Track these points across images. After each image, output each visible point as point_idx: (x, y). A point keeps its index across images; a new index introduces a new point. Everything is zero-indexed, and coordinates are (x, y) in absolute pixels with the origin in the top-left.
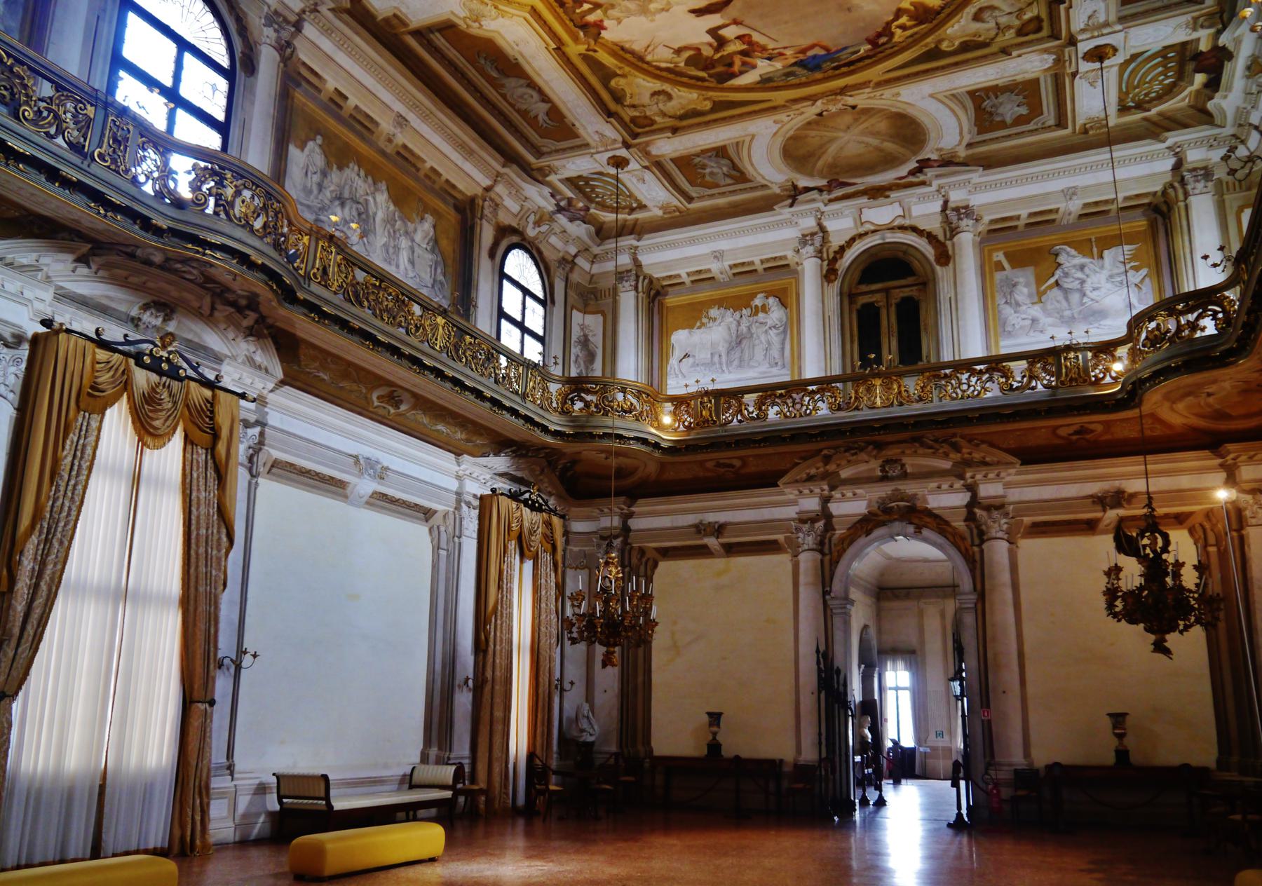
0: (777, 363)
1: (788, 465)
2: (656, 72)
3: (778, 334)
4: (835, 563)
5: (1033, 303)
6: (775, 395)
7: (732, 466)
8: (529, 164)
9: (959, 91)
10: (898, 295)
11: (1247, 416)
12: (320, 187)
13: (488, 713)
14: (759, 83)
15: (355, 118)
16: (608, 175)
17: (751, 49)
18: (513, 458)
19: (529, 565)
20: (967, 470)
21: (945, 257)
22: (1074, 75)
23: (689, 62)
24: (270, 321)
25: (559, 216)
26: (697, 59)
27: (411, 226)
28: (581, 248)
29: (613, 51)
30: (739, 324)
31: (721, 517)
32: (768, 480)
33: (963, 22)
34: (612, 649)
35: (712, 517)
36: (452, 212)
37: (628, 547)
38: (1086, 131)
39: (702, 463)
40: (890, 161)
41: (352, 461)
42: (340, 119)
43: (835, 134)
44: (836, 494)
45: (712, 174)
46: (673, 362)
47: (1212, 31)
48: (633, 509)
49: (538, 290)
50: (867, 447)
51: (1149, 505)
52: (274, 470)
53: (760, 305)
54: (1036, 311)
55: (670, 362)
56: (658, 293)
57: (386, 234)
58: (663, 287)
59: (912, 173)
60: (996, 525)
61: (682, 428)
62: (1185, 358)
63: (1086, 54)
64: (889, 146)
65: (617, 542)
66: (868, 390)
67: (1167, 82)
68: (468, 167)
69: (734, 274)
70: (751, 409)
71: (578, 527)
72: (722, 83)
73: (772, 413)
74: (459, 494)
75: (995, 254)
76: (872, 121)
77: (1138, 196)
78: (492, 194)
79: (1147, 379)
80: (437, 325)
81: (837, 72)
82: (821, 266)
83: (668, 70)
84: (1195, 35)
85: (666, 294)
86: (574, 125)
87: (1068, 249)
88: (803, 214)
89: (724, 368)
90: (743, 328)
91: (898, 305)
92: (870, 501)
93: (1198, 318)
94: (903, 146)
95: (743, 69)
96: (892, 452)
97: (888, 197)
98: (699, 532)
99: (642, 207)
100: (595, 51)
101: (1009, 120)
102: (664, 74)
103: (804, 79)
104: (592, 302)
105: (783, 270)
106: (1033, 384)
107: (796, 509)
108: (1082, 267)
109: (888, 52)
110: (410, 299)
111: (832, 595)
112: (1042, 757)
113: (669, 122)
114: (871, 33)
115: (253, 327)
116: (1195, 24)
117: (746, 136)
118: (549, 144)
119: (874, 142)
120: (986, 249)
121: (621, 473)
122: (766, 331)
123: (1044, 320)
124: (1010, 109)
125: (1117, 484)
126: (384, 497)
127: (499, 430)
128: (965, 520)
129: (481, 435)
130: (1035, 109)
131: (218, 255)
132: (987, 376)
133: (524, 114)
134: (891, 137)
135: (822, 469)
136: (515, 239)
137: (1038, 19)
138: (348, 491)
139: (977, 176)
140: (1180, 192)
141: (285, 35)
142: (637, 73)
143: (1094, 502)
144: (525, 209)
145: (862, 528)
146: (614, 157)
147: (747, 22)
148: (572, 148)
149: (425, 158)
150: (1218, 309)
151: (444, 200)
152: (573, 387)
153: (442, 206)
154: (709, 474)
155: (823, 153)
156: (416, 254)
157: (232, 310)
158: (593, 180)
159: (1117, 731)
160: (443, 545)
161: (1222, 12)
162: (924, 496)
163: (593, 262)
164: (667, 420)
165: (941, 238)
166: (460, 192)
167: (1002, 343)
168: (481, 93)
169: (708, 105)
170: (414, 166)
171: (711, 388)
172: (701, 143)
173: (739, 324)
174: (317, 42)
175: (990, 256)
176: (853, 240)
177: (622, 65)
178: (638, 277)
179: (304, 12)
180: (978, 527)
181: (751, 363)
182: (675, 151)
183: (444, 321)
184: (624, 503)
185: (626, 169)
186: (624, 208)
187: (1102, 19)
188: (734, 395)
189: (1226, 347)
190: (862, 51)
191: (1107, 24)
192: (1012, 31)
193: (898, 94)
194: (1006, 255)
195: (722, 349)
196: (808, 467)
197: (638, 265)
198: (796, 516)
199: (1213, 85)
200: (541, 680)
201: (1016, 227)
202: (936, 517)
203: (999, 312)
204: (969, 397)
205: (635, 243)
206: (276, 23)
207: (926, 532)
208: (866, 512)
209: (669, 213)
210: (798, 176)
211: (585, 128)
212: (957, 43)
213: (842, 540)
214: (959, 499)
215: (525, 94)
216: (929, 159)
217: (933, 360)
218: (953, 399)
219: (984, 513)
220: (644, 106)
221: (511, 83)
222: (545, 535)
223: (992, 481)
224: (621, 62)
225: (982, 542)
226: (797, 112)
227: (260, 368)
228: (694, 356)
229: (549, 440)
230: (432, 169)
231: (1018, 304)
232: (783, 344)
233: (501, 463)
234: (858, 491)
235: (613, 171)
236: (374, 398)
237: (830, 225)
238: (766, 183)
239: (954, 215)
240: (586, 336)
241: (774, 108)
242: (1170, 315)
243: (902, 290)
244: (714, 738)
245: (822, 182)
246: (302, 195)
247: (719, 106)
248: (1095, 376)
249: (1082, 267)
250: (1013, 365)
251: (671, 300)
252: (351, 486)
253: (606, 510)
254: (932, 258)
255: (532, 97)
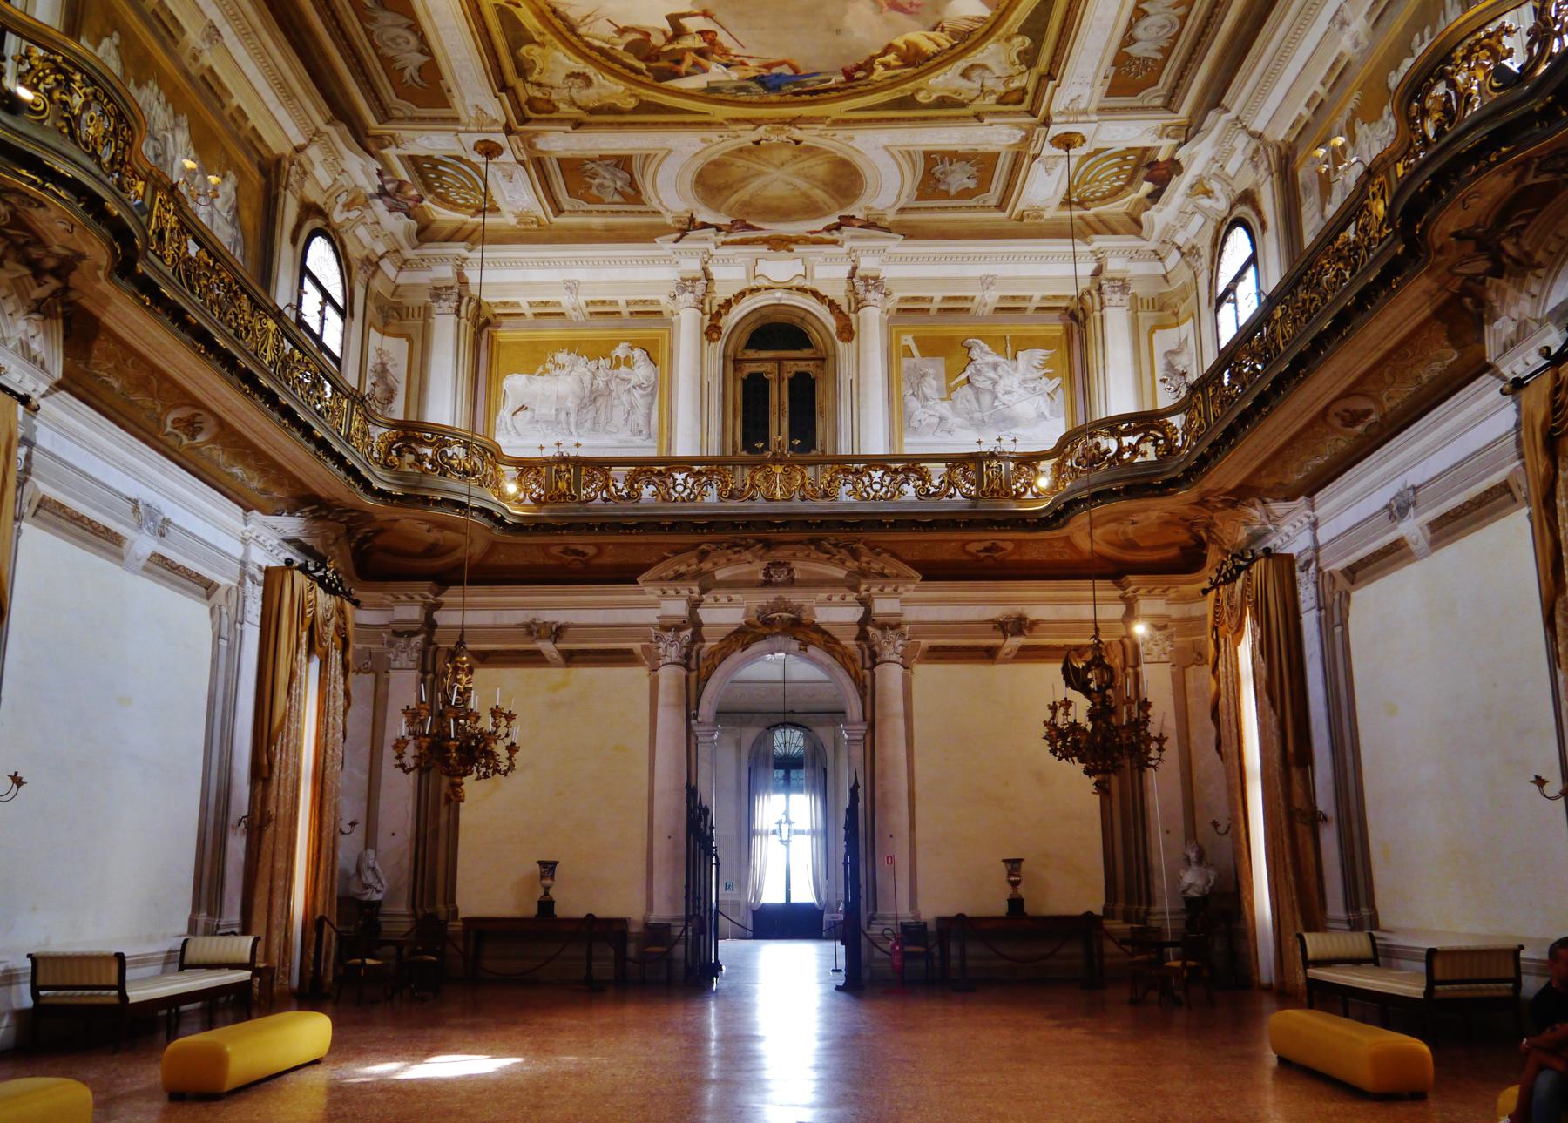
0: (640, 432)
1: (655, 559)
2: (584, 50)
3: (644, 396)
4: (704, 680)
5: (942, 399)
6: (652, 472)
7: (582, 554)
8: (365, 127)
9: (916, 149)
10: (792, 368)
11: (1154, 548)
13: (269, 864)
14: (703, 90)
15: (157, 16)
16: (468, 163)
17: (710, 48)
18: (309, 519)
19: (315, 665)
20: (863, 581)
21: (847, 332)
22: (1035, 157)
23: (629, 47)
24: (73, 295)
25: (378, 201)
26: (642, 46)
28: (392, 248)
29: (541, 11)
30: (594, 377)
31: (561, 617)
32: (625, 575)
33: (949, 75)
34: (458, 780)
35: (548, 616)
36: (257, 174)
37: (432, 647)
38: (1021, 219)
39: (545, 548)
40: (811, 209)
41: (130, 506)
43: (764, 168)
44: (709, 599)
45: (601, 185)
46: (505, 413)
47: (1175, 142)
48: (442, 598)
49: (337, 294)
50: (754, 545)
51: (1096, 636)
52: (41, 512)
53: (622, 357)
54: (944, 408)
55: (501, 413)
56: (488, 323)
58: (494, 315)
59: (828, 229)
60: (890, 647)
61: (528, 501)
62: (1128, 483)
63: (1054, 138)
64: (819, 194)
65: (418, 640)
66: (766, 478)
67: (1116, 184)
68: (282, 115)
69: (591, 314)
70: (620, 485)
71: (365, 616)
72: (660, 81)
73: (647, 492)
74: (243, 563)
75: (904, 337)
76: (812, 162)
77: (1055, 297)
78: (302, 157)
79: (1084, 501)
80: (265, 331)
81: (796, 98)
82: (702, 320)
83: (601, 50)
84: (1158, 143)
85: (499, 325)
86: (449, 91)
87: (982, 344)
88: (686, 254)
89: (573, 430)
90: (600, 382)
91: (791, 380)
92: (748, 609)
93: (1138, 442)
94: (833, 197)
95: (691, 70)
96: (780, 554)
97: (792, 250)
98: (530, 633)
99: (495, 210)
100: (518, 6)
101: (953, 191)
102: (594, 54)
103: (755, 98)
104: (394, 321)
105: (654, 317)
106: (952, 491)
107: (658, 613)
108: (995, 367)
109: (861, 88)
110: (241, 288)
111: (699, 719)
112: (931, 909)
113: (575, 112)
114: (850, 64)
115: (44, 300)
116: (1163, 133)
117: (662, 149)
118: (407, 108)
119: (804, 185)
120: (894, 330)
121: (433, 550)
122: (629, 391)
123: (954, 420)
124: (959, 178)
125: (1019, 609)
126: (160, 561)
127: (305, 479)
128: (856, 639)
129: (282, 485)
130: (984, 185)
131: (62, 193)
132: (902, 476)
133: (387, 62)
134: (825, 184)
135: (694, 567)
136: (318, 223)
137: (1024, 90)
138: (126, 546)
139: (895, 244)
140: (1097, 300)
142: (559, 45)
143: (995, 628)
144: (338, 185)
145: (738, 640)
146: (486, 141)
147: (719, 16)
148: (434, 120)
149: (233, 92)
150: (1160, 435)
151: (248, 154)
152: (401, 434)
153: (245, 160)
154: (552, 562)
155: (742, 187)
157: (26, 271)
158: (445, 164)
159: (1012, 879)
160: (224, 633)
161: (1189, 126)
162: (811, 608)
163: (401, 268)
164: (512, 488)
165: (845, 308)
166: (267, 146)
167: (906, 440)
168: (338, 22)
169: (633, 103)
170: (219, 99)
171: (573, 453)
172: (603, 146)
173: (594, 377)
175: (898, 338)
176: (742, 294)
177: (543, 30)
178: (461, 297)
180: (871, 648)
181: (609, 428)
182: (567, 150)
183: (275, 326)
184: (430, 591)
185: (495, 160)
186: (468, 207)
187: (1083, 105)
188: (601, 465)
189: (1171, 476)
190: (833, 82)
191: (1085, 112)
192: (994, 97)
193: (852, 138)
194: (916, 340)
195: (571, 405)
196: (679, 563)
197: (463, 282)
198: (657, 621)
199: (1155, 196)
200: (325, 819)
201: (928, 310)
202: (824, 632)
203: (905, 404)
204: (881, 498)
205: (464, 253)
207: (812, 650)
208: (743, 621)
209: (525, 223)
210: (702, 208)
211: (462, 96)
212: (934, 96)
213: (713, 654)
214: (853, 614)
215: (399, 37)
216: (853, 217)
217: (829, 451)
218: (864, 499)
219: (878, 633)
220: (552, 87)
221: (386, 18)
222: (337, 627)
223: (888, 596)
224: (545, 27)
225: (875, 664)
226: (731, 134)
227: (34, 360)
228: (533, 410)
229: (369, 502)
230: (239, 109)
231: (926, 398)
232: (650, 408)
233: (292, 525)
234: (734, 596)
235: (477, 159)
236: (169, 422)
237: (717, 272)
238: (661, 209)
239: (862, 284)
240: (383, 365)
241: (709, 124)
242: (1112, 435)
243: (796, 362)
244: (546, 894)
245: (724, 220)
247: (645, 107)
248: (1016, 490)
249: (995, 367)
250: (930, 467)
251: (505, 334)
252: (128, 543)
253: (403, 598)
254: (833, 330)
255: (408, 43)
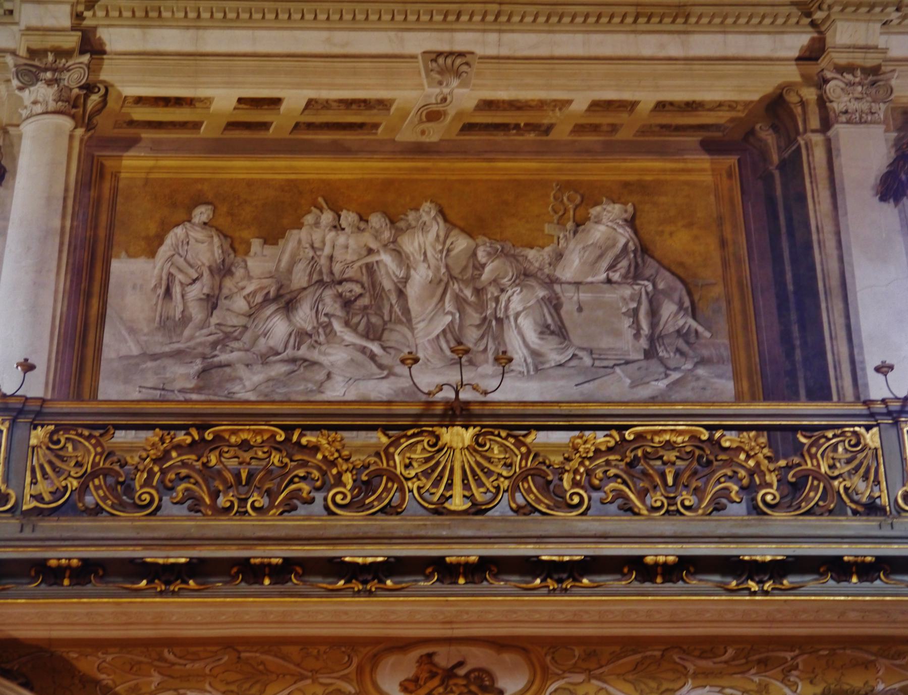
12: (212, 302)
27: (535, 257)
42: (217, 148)
57: (449, 305)
141: (74, 78)
156: (568, 309)
166: (720, 105)
174: (150, 47)
179: (79, 16)
206: (46, 70)
246: (159, 338)
